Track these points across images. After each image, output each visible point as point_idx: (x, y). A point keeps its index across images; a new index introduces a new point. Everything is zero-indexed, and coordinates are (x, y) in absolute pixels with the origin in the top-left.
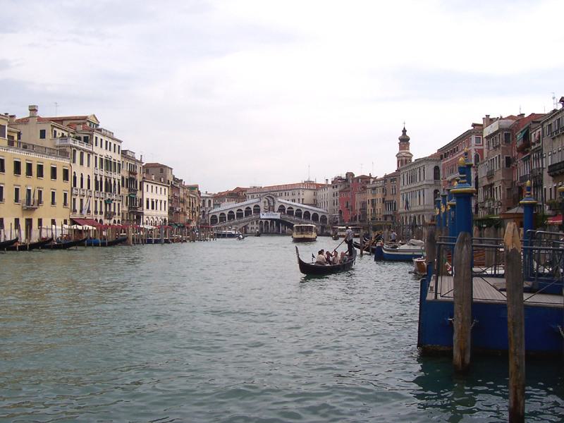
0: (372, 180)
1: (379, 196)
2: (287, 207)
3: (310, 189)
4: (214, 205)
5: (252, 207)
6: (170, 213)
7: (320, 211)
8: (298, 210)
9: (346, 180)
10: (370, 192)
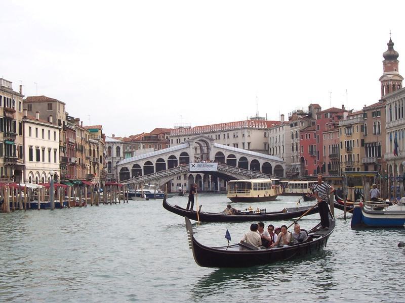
0: (345, 115)
1: (356, 136)
2: (226, 154)
3: (259, 129)
4: (124, 153)
5: (178, 155)
6: (62, 166)
7: (274, 159)
9: (310, 115)
10: (343, 129)
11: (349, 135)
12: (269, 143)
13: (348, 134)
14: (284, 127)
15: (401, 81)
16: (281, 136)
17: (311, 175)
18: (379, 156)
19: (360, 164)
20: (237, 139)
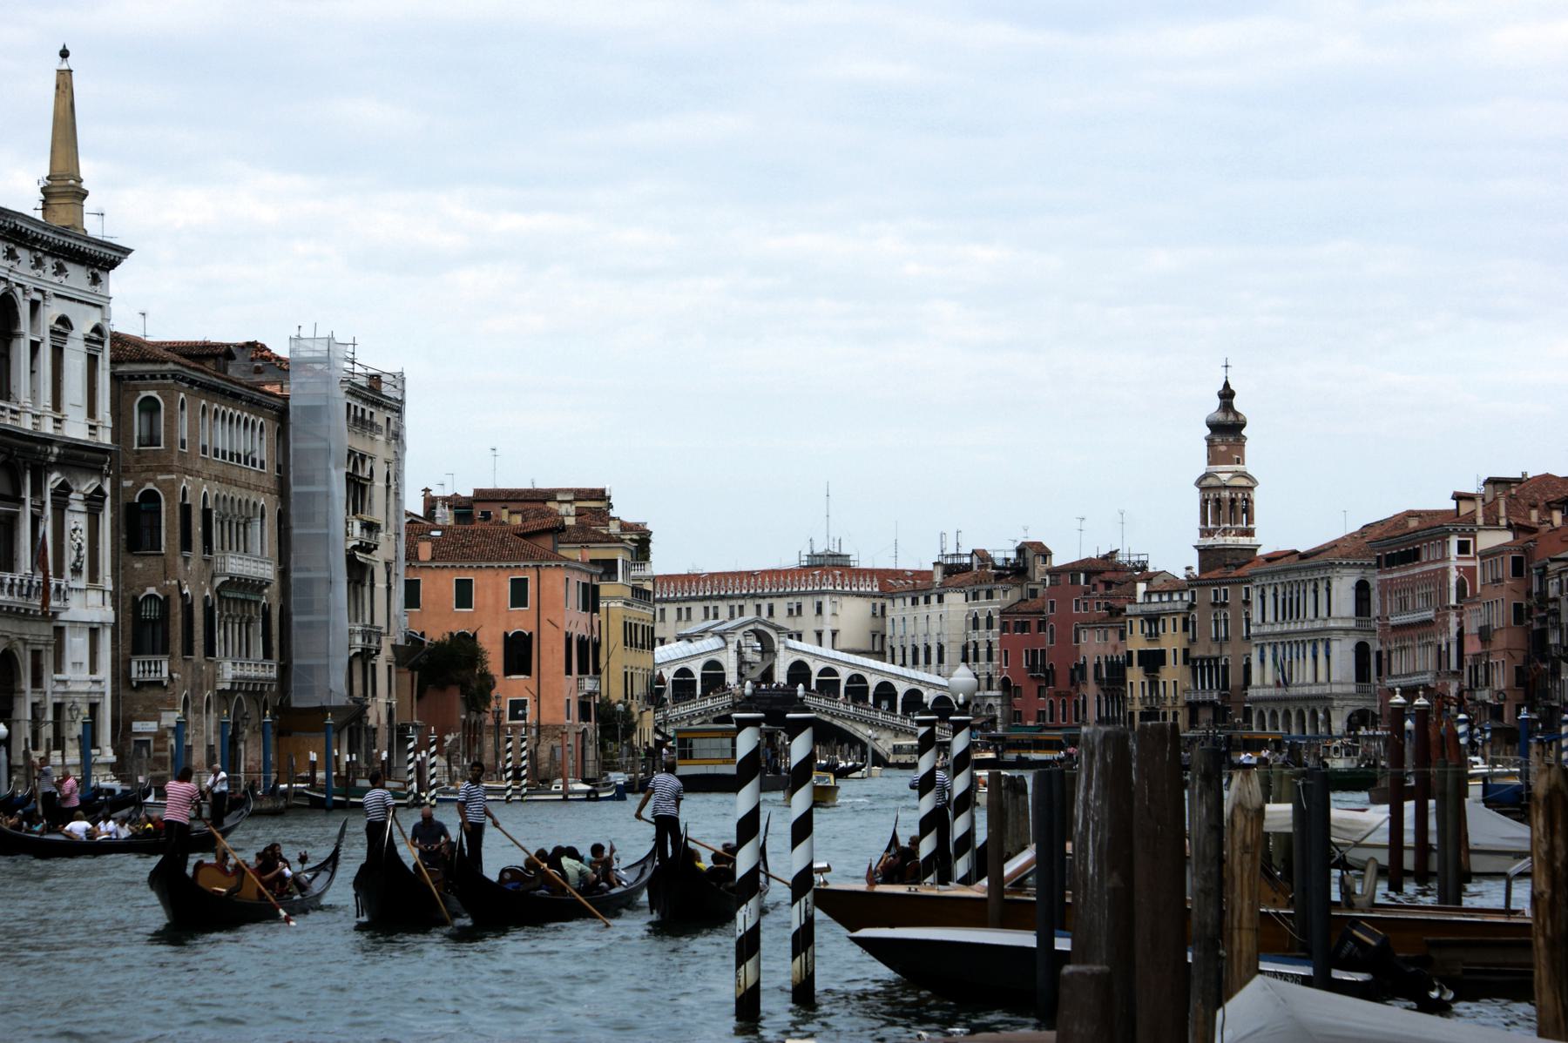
2: (816, 667)
3: (859, 595)
5: (697, 667)
8: (850, 680)
10: (1137, 624)
11: (1153, 636)
12: (889, 633)
13: (1151, 634)
14: (947, 597)
15: (1251, 488)
16: (934, 618)
17: (1030, 723)
18: (1226, 687)
19: (1180, 703)
20: (799, 619)
